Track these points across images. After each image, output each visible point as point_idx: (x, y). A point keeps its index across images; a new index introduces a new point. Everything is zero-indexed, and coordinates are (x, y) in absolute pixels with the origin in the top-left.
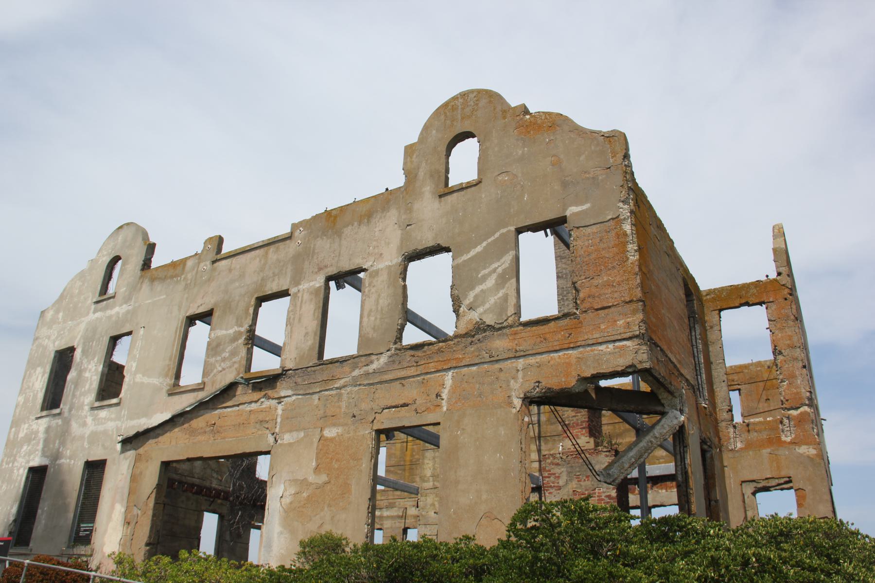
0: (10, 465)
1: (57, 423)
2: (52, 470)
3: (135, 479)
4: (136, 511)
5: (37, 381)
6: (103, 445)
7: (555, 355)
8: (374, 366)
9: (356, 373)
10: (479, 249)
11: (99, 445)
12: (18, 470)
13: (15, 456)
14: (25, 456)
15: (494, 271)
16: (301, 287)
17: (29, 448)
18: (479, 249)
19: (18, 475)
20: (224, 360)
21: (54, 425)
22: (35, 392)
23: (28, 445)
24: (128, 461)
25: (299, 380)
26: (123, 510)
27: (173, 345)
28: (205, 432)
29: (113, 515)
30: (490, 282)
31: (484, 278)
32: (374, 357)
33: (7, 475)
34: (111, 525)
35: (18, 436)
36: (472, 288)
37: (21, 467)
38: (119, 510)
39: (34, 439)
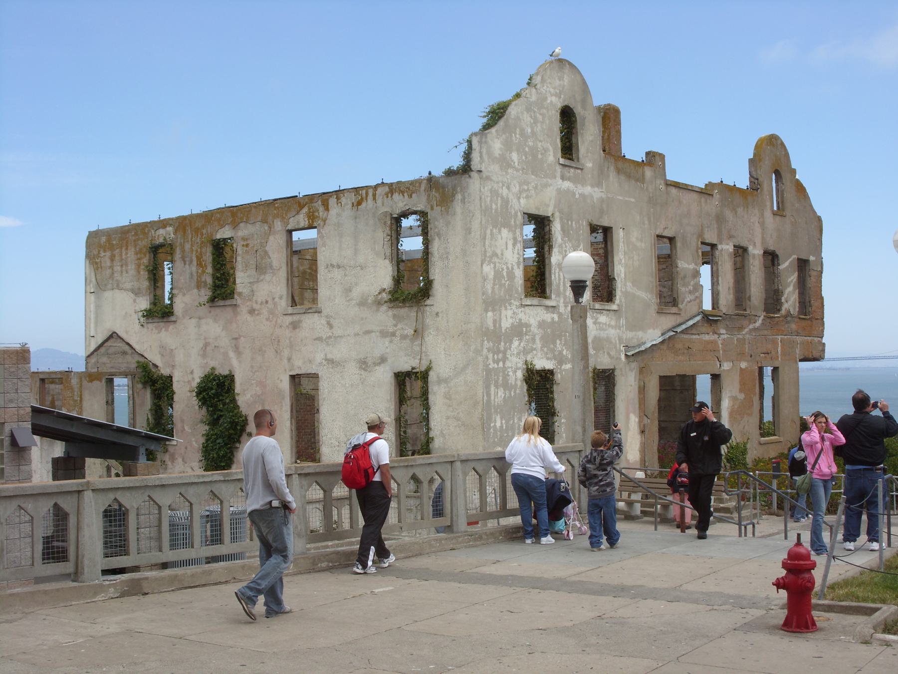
0: (501, 364)
1: (553, 319)
2: (559, 376)
3: (642, 390)
4: (646, 421)
5: (507, 249)
6: (609, 354)
7: (805, 338)
8: (758, 324)
9: (751, 327)
10: (787, 264)
11: (604, 352)
12: (515, 372)
13: (504, 353)
14: (518, 354)
15: (792, 281)
16: (723, 246)
17: (522, 345)
18: (787, 264)
19: (516, 379)
20: (690, 292)
21: (549, 320)
22: (510, 266)
23: (521, 340)
24: (634, 373)
25: (728, 323)
26: (637, 420)
27: (652, 261)
28: (684, 353)
29: (630, 425)
30: (790, 289)
31: (789, 286)
32: (757, 318)
33: (501, 378)
34: (630, 434)
35: (500, 325)
36: (786, 289)
37: (518, 369)
38: (634, 420)
39: (526, 334)
